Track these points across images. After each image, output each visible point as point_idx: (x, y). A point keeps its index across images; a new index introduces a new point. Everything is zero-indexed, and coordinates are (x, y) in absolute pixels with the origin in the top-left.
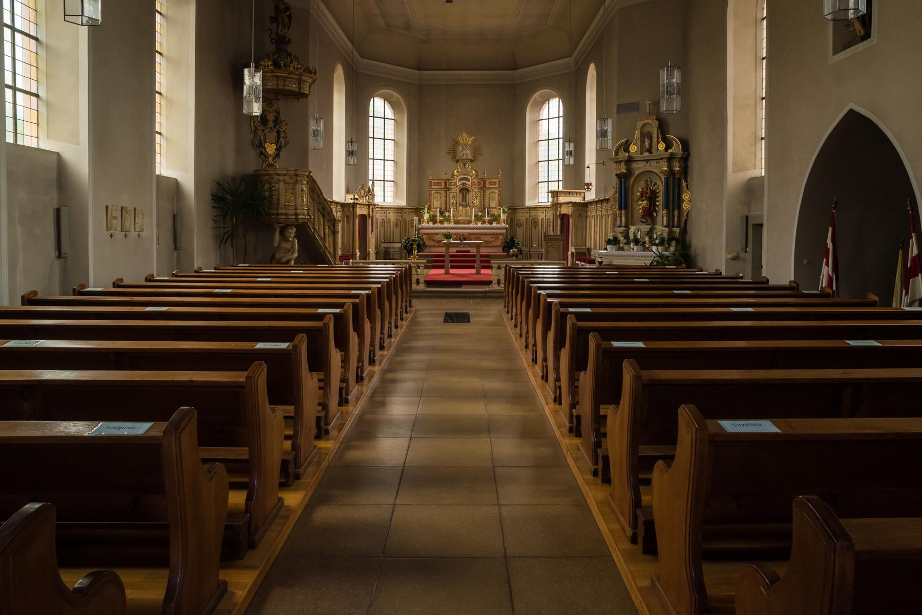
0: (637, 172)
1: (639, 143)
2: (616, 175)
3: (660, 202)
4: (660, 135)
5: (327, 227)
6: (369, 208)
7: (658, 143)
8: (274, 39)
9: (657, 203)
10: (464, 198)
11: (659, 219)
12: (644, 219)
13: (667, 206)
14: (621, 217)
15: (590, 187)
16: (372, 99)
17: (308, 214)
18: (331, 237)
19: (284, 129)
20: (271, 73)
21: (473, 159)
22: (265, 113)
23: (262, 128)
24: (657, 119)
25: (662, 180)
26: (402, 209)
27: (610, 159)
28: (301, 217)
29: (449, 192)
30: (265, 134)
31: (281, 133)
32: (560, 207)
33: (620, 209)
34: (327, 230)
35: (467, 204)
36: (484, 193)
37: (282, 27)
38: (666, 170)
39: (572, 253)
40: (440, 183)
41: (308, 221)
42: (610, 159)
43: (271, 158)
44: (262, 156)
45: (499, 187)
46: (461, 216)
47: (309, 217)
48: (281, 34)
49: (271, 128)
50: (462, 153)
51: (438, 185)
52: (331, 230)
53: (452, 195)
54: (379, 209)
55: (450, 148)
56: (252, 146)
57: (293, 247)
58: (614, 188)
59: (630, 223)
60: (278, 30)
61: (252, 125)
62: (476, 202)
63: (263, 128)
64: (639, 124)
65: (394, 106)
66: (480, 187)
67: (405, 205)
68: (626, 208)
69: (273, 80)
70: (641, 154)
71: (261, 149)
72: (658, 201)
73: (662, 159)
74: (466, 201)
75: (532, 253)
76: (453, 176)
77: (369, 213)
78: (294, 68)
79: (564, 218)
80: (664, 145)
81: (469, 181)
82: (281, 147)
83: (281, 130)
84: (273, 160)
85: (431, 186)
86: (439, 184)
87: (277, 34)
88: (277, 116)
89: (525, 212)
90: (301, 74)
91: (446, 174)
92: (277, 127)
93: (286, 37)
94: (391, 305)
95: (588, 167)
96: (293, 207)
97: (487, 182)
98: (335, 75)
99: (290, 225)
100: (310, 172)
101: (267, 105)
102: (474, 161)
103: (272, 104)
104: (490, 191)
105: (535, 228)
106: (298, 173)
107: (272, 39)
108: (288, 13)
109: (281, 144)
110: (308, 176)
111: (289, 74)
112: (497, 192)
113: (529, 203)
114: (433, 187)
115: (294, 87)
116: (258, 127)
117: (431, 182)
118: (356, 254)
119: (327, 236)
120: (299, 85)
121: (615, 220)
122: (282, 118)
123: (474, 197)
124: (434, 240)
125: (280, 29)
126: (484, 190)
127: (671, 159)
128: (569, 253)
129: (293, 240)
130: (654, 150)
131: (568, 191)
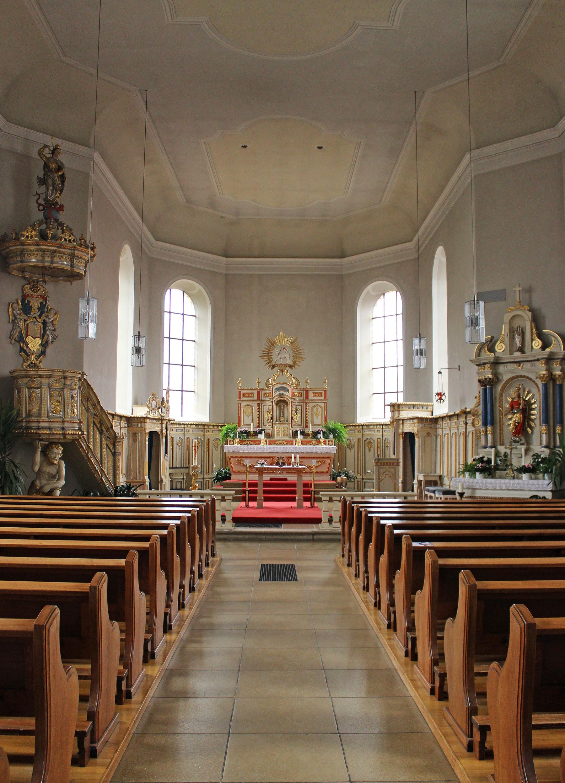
0: (506, 378)
1: (507, 340)
2: (479, 381)
3: (536, 413)
4: (534, 331)
5: (105, 446)
6: (162, 423)
7: (532, 340)
8: (42, 205)
9: (533, 417)
10: (281, 413)
11: (535, 438)
12: (517, 437)
13: (546, 421)
14: (486, 435)
15: (443, 398)
16: (169, 290)
17: (80, 429)
18: (111, 458)
19: (52, 319)
20: (36, 245)
21: (292, 364)
22: (28, 298)
23: (24, 317)
24: (530, 310)
25: (538, 388)
26: (204, 425)
27: (471, 361)
28: (70, 433)
29: (263, 405)
30: (28, 325)
31: (48, 325)
32: (402, 424)
33: (485, 424)
34: (105, 450)
35: (286, 420)
36: (306, 406)
37: (53, 190)
38: (544, 375)
39: (420, 482)
40: (252, 394)
41: (80, 438)
42: (471, 361)
43: (34, 357)
44: (23, 353)
46: (278, 434)
47: (80, 433)
48: (51, 199)
49: (35, 318)
51: (249, 397)
52: (109, 449)
53: (266, 409)
54: (176, 426)
56: (10, 340)
57: (59, 472)
58: (476, 398)
59: (499, 444)
60: (47, 195)
61: (10, 313)
62: (297, 417)
63: (25, 318)
64: (507, 317)
65: (195, 298)
67: (208, 421)
68: (493, 423)
69: (37, 255)
70: (510, 355)
71: (21, 344)
72: (533, 415)
73: (538, 360)
74: (283, 416)
75: (365, 481)
76: (267, 385)
77: (162, 430)
78: (65, 240)
79: (410, 437)
80: (540, 342)
81: (288, 392)
82: (47, 342)
83: (48, 320)
84: (36, 359)
85: (240, 397)
86: (250, 395)
87: (46, 199)
88: (44, 303)
89: (356, 431)
90: (74, 248)
91: (259, 382)
92: (43, 317)
93: (57, 203)
94: (183, 560)
95: (440, 373)
96: (60, 420)
97: (310, 393)
98: (121, 259)
99: (56, 443)
100: (83, 374)
101: (31, 289)
102: (294, 366)
103: (37, 287)
104: (314, 404)
105: (370, 450)
106: (67, 374)
107: (40, 205)
108: (62, 173)
109: (47, 338)
110: (80, 380)
111: (58, 247)
112: (323, 405)
113: (361, 419)
114: (242, 399)
115: (65, 264)
116: (18, 317)
117: (240, 392)
118: (145, 482)
119: (105, 458)
120: (72, 262)
121: (478, 439)
122: (50, 304)
123: (294, 412)
125: (50, 192)
126: (306, 403)
127: (549, 360)
128: (415, 482)
129: (59, 463)
130: (527, 349)
131: (412, 403)
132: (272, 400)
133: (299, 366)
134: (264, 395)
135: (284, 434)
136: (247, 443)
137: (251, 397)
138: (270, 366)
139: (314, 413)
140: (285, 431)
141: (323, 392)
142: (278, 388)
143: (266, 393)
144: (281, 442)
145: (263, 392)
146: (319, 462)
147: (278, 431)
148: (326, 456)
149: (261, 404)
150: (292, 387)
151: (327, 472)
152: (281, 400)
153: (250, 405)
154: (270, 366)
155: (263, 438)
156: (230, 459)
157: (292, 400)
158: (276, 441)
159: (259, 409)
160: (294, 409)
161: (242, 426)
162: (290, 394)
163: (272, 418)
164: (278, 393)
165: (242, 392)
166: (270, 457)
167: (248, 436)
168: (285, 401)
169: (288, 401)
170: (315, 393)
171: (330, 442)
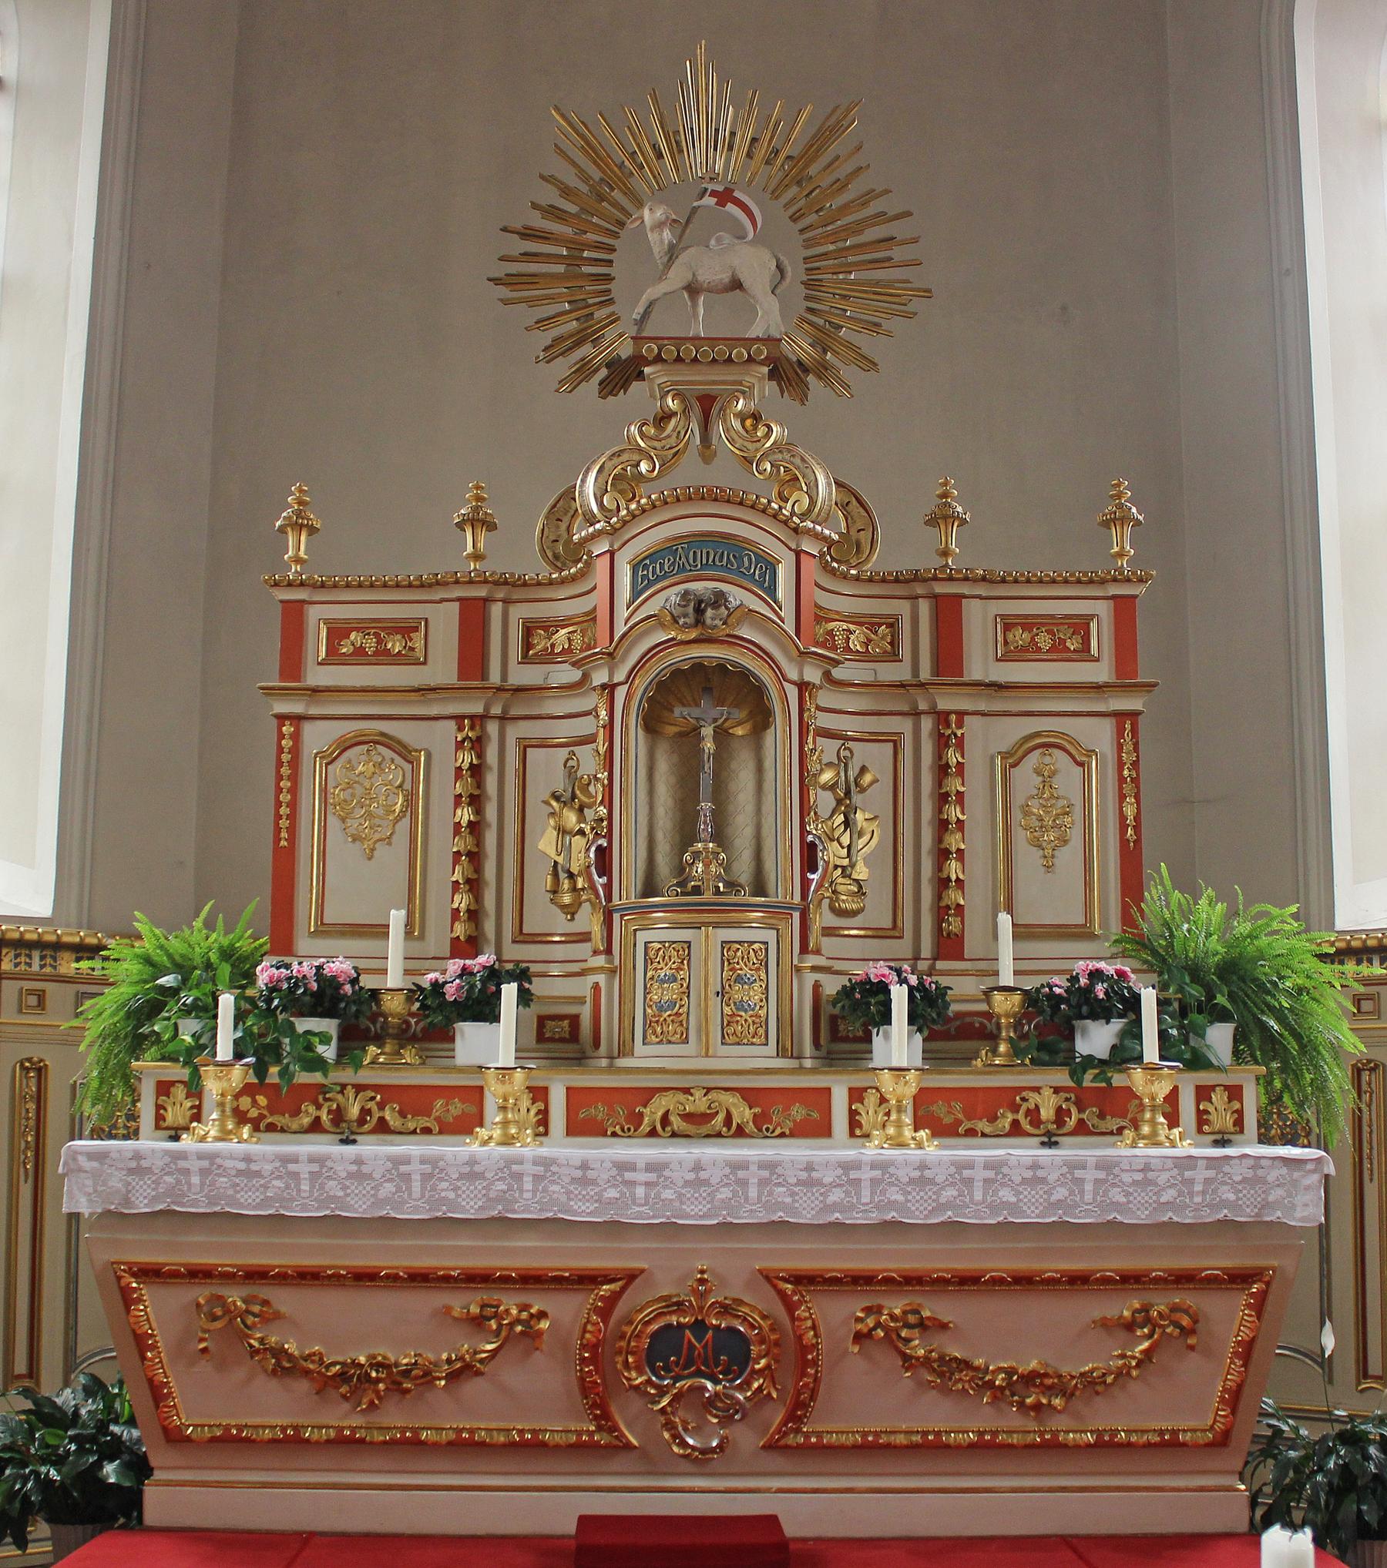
21: (800, 348)
29: (514, 731)
35: (743, 871)
36: (942, 742)
40: (406, 629)
45: (1126, 678)
50: (677, 277)
51: (383, 656)
55: (528, 234)
66: (890, 672)
74: (719, 836)
81: (772, 590)
85: (292, 662)
91: (479, 521)
104: (1016, 729)
112: (1100, 736)
114: (317, 676)
117: (293, 616)
123: (824, 801)
124: (285, 1367)
132: (600, 677)
133: (869, 364)
134: (527, 645)
135: (727, 1022)
136: (338, 1116)
137: (398, 659)
138: (584, 371)
139: (1017, 815)
140: (738, 992)
141: (1103, 610)
142: (669, 549)
143: (550, 626)
144: (698, 1103)
145: (519, 613)
146: (1130, 1326)
147: (671, 992)
148: (1215, 1262)
149: (492, 728)
150: (809, 546)
151: (1223, 1440)
152: (699, 667)
153: (386, 741)
154: (584, 371)
155: (506, 1056)
156: (128, 1299)
157: (813, 675)
158: (648, 1094)
159: (477, 771)
160: (827, 776)
161: (303, 944)
162: (788, 613)
163: (604, 855)
164: (666, 598)
165: (314, 613)
166: (587, 1280)
167: (353, 1039)
168: (744, 675)
169: (766, 676)
170: (1029, 623)
171: (1219, 1098)
